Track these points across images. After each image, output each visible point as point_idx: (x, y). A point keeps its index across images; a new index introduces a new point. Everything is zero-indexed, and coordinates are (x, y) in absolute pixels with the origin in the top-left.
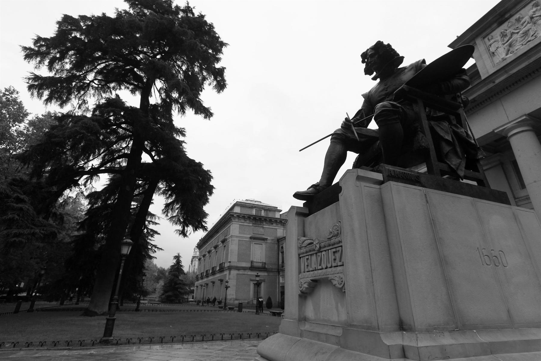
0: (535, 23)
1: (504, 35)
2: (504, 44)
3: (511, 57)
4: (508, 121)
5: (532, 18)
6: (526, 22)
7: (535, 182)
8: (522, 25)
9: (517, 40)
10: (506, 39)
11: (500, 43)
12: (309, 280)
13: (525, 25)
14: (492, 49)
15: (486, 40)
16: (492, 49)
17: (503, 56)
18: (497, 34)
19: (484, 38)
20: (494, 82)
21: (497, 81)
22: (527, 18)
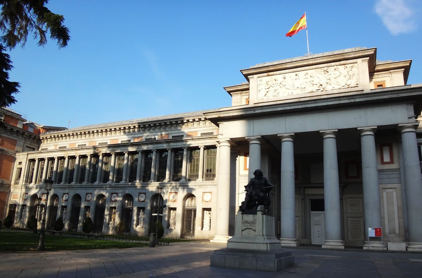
4: (252, 135)
10: (268, 87)
12: (245, 228)
13: (277, 85)
14: (260, 88)
16: (260, 88)
20: (255, 111)
21: (257, 112)
22: (278, 82)
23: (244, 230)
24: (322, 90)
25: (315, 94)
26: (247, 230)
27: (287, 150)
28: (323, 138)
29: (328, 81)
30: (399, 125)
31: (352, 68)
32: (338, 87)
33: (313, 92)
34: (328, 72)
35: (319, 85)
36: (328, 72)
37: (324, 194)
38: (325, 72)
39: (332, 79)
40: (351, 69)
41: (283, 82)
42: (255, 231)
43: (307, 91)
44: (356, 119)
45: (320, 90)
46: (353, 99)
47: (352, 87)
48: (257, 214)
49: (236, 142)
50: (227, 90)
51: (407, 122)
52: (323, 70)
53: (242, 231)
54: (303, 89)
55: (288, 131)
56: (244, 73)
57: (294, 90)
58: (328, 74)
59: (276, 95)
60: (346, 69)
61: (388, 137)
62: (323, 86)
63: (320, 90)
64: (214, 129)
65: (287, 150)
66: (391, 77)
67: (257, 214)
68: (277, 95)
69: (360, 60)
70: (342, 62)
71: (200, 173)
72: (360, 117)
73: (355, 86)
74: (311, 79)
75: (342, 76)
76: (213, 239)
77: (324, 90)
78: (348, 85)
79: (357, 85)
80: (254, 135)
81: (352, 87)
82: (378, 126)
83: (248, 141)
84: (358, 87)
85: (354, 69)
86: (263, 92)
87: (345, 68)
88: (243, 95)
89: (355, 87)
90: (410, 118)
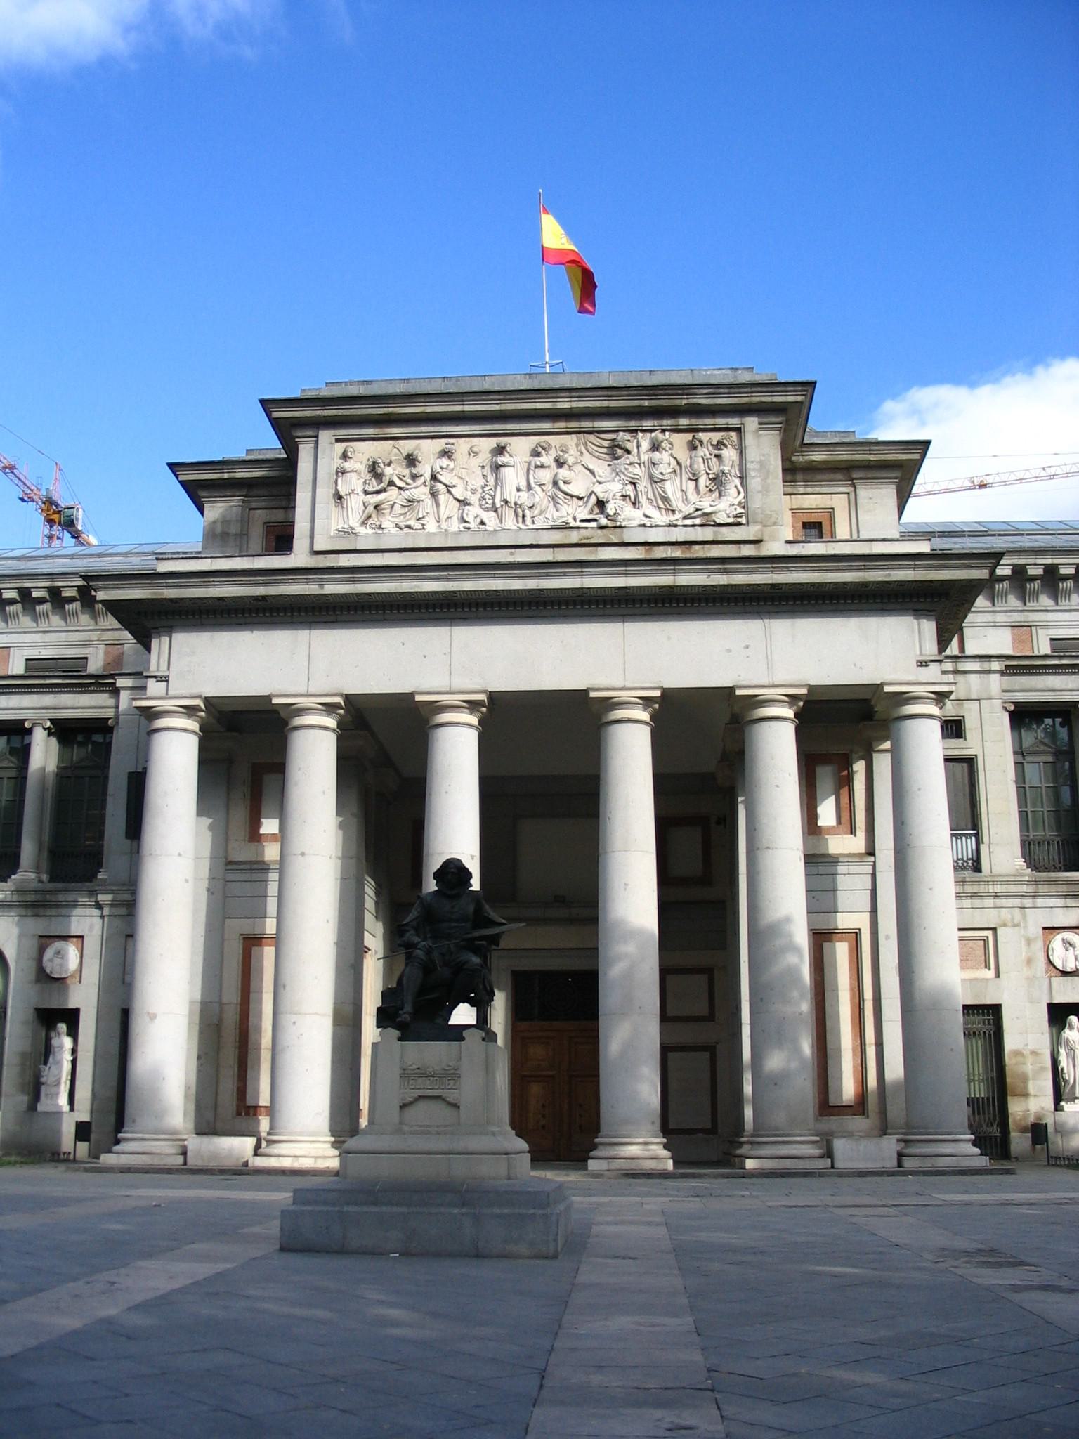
0: (434, 494)
1: (374, 470)
2: (366, 493)
3: (366, 537)
4: (303, 690)
5: (434, 478)
6: (421, 480)
7: (303, 854)
8: (414, 477)
9: (392, 506)
11: (359, 487)
15: (340, 448)
17: (354, 521)
18: (365, 451)
19: (337, 441)
20: (321, 586)
23: (411, 1103)
25: (574, 537)
26: (422, 1107)
27: (457, 764)
28: (600, 719)
29: (630, 490)
30: (887, 689)
33: (566, 527)
34: (628, 452)
35: (593, 500)
37: (597, 949)
38: (619, 452)
41: (445, 473)
42: (456, 1106)
43: (540, 523)
44: (729, 651)
45: (595, 520)
46: (725, 571)
48: (463, 1039)
49: (220, 712)
50: (181, 478)
51: (911, 678)
53: (403, 1106)
54: (527, 512)
55: (458, 683)
56: (276, 415)
57: (487, 510)
58: (632, 458)
59: (412, 523)
60: (702, 451)
61: (844, 727)
62: (610, 509)
63: (595, 520)
64: (88, 644)
65: (457, 764)
66: (852, 495)
67: (463, 1039)
68: (417, 525)
69: (751, 423)
70: (684, 422)
71: (28, 849)
72: (747, 647)
73: (731, 520)
74: (563, 473)
76: (110, 1152)
80: (312, 691)
82: (811, 688)
83: (283, 714)
84: (739, 524)
86: (355, 504)
88: (254, 505)
90: (922, 664)
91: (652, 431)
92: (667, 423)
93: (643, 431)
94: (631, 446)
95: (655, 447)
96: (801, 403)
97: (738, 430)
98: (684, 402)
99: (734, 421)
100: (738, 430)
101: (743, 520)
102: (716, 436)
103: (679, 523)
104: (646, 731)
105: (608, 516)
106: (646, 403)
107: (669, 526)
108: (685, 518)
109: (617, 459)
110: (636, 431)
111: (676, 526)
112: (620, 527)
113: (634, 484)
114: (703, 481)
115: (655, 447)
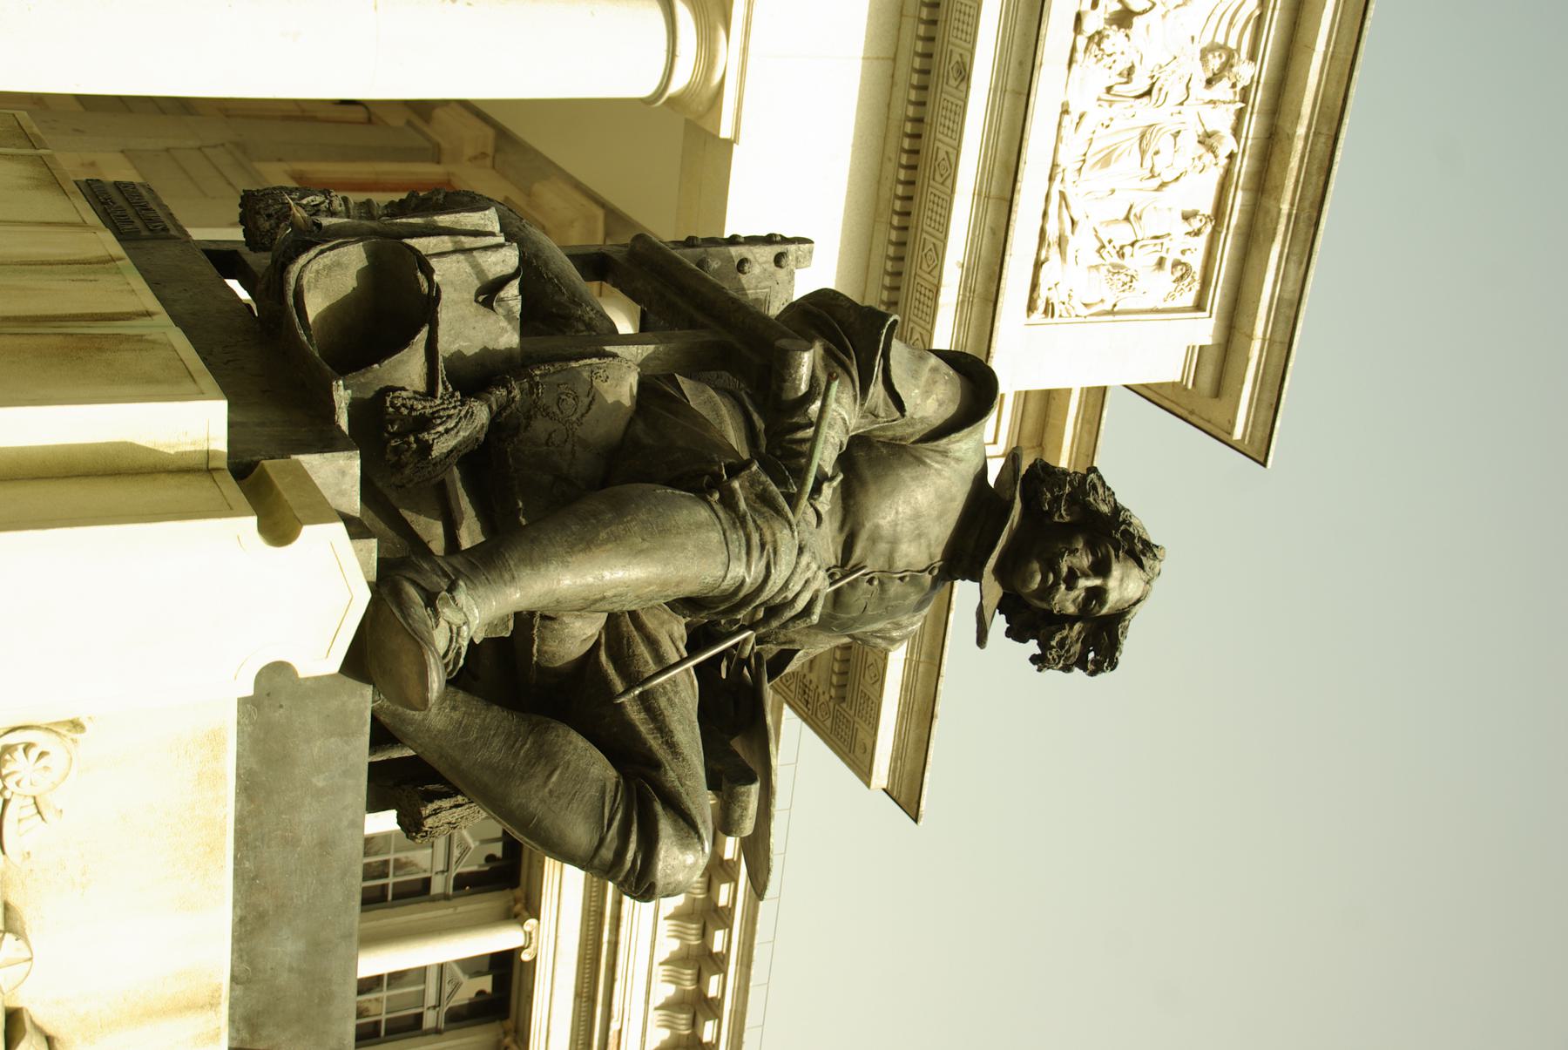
24: (1093, 23)
29: (1140, 83)
31: (1178, 273)
32: (1068, 159)
34: (1209, 82)
36: (1209, 82)
38: (1215, 63)
39: (1146, 112)
40: (1168, 265)
47: (1038, 265)
52: (1232, 44)
58: (1198, 85)
69: (1205, 330)
70: (1238, 200)
73: (1043, 293)
75: (1143, 198)
77: (1082, 41)
78: (1061, 242)
79: (1041, 305)
81: (1038, 265)
84: (1031, 307)
85: (1158, 288)
87: (1196, 224)
89: (1034, 286)
91: (1236, 132)
92: (1244, 166)
93: (1240, 114)
94: (1222, 90)
95: (1207, 140)
96: (1230, 433)
97: (1199, 306)
98: (1285, 207)
99: (1217, 297)
100: (1199, 306)
101: (1038, 315)
102: (1196, 261)
103: (1057, 186)
104: (643, 87)
105: (1098, 38)
106: (1301, 130)
107: (1054, 166)
108: (1063, 195)
109: (1204, 54)
110: (1244, 99)
111: (1051, 179)
112: (1071, 62)
113: (1148, 93)
114: (1123, 234)
115: (1207, 140)
